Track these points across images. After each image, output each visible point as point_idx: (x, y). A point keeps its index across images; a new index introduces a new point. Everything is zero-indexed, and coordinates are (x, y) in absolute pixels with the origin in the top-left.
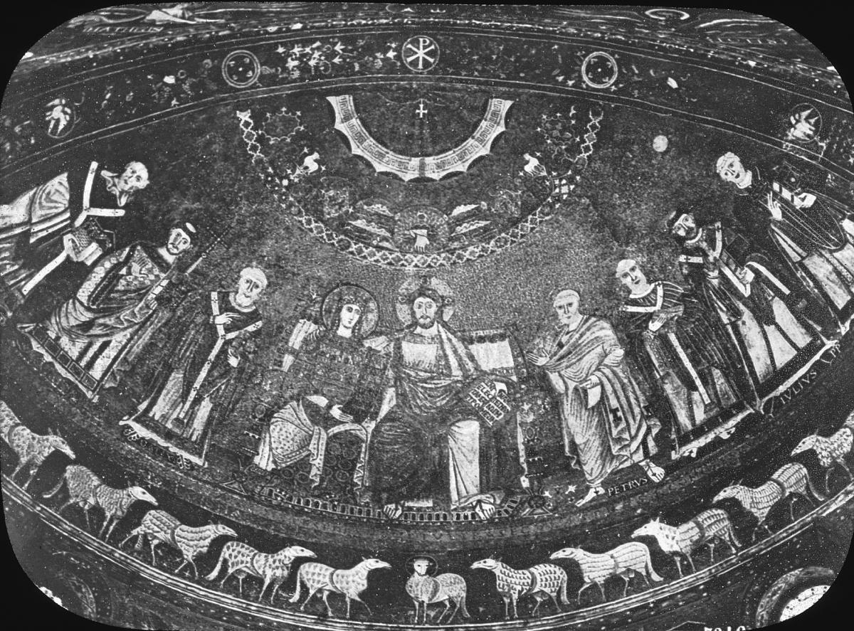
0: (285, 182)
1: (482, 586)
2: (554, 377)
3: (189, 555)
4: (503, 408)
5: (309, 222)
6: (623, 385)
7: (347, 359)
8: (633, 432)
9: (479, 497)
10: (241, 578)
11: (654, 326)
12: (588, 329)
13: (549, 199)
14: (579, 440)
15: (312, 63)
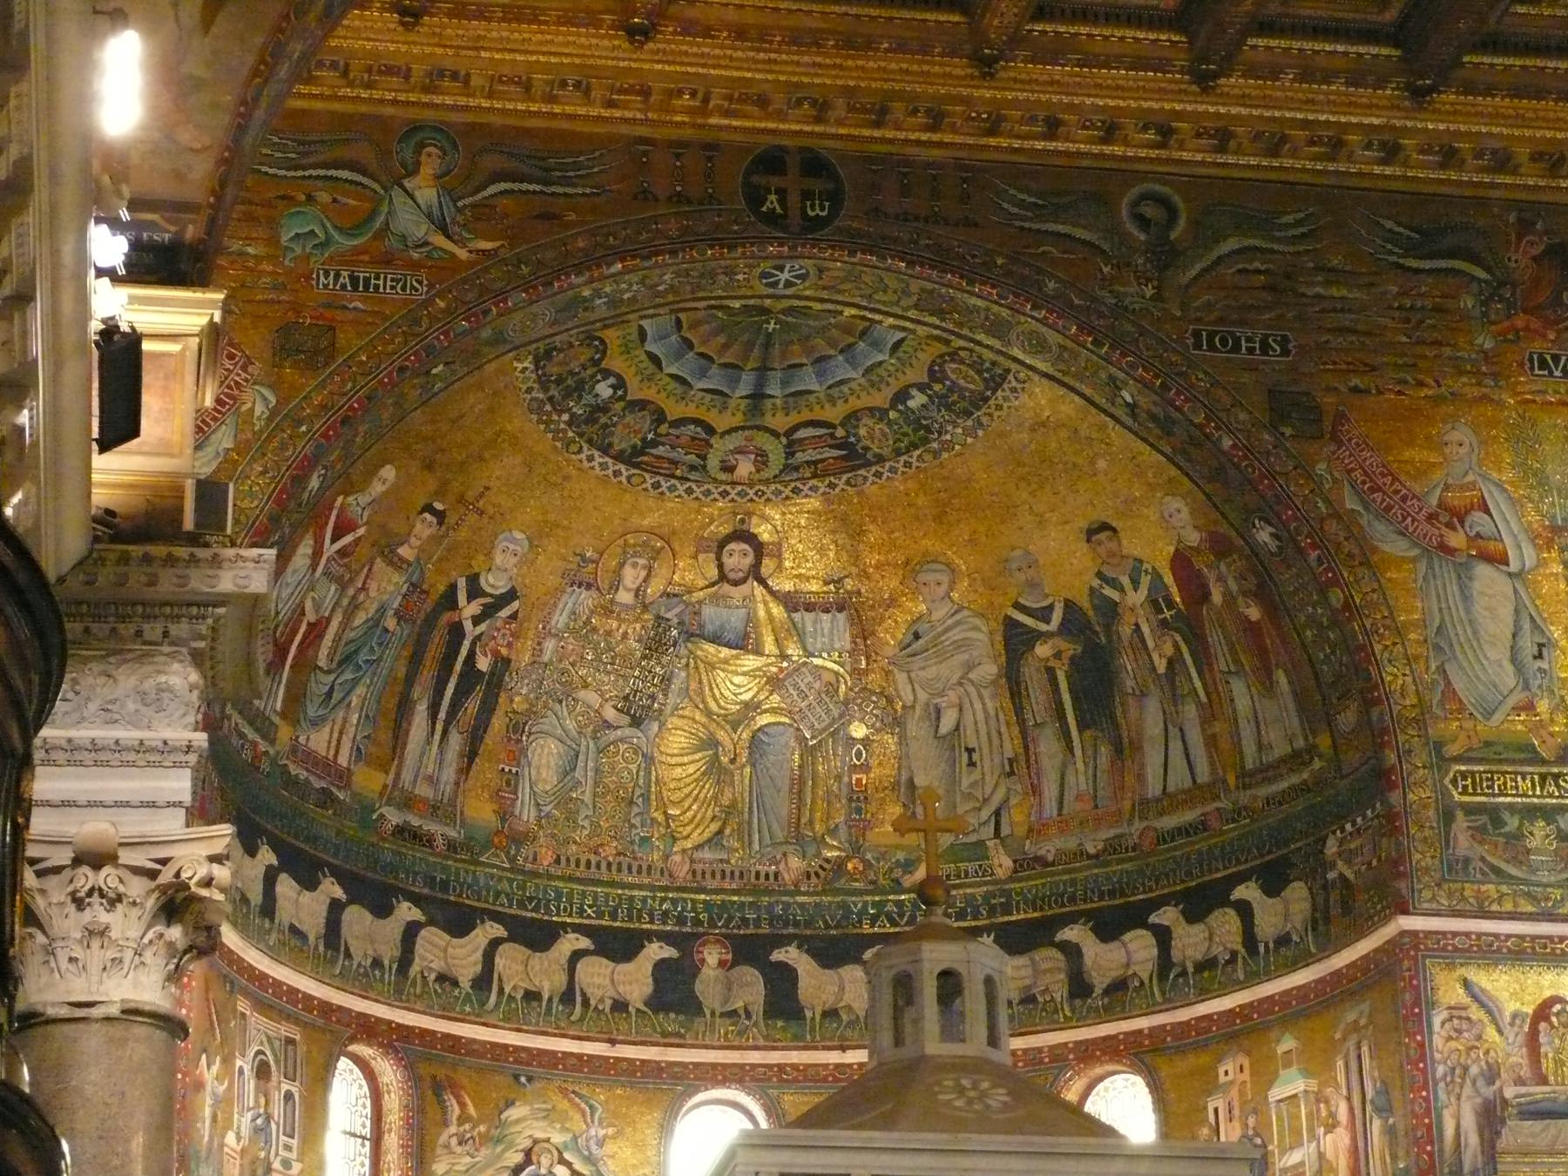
0: (565, 417)
1: (782, 984)
2: (901, 677)
3: (465, 984)
4: (828, 712)
5: (590, 459)
6: (987, 718)
7: (626, 633)
8: (988, 790)
9: (784, 848)
10: (519, 997)
11: (1043, 650)
12: (958, 623)
13: (935, 445)
14: (916, 781)
15: (626, 296)
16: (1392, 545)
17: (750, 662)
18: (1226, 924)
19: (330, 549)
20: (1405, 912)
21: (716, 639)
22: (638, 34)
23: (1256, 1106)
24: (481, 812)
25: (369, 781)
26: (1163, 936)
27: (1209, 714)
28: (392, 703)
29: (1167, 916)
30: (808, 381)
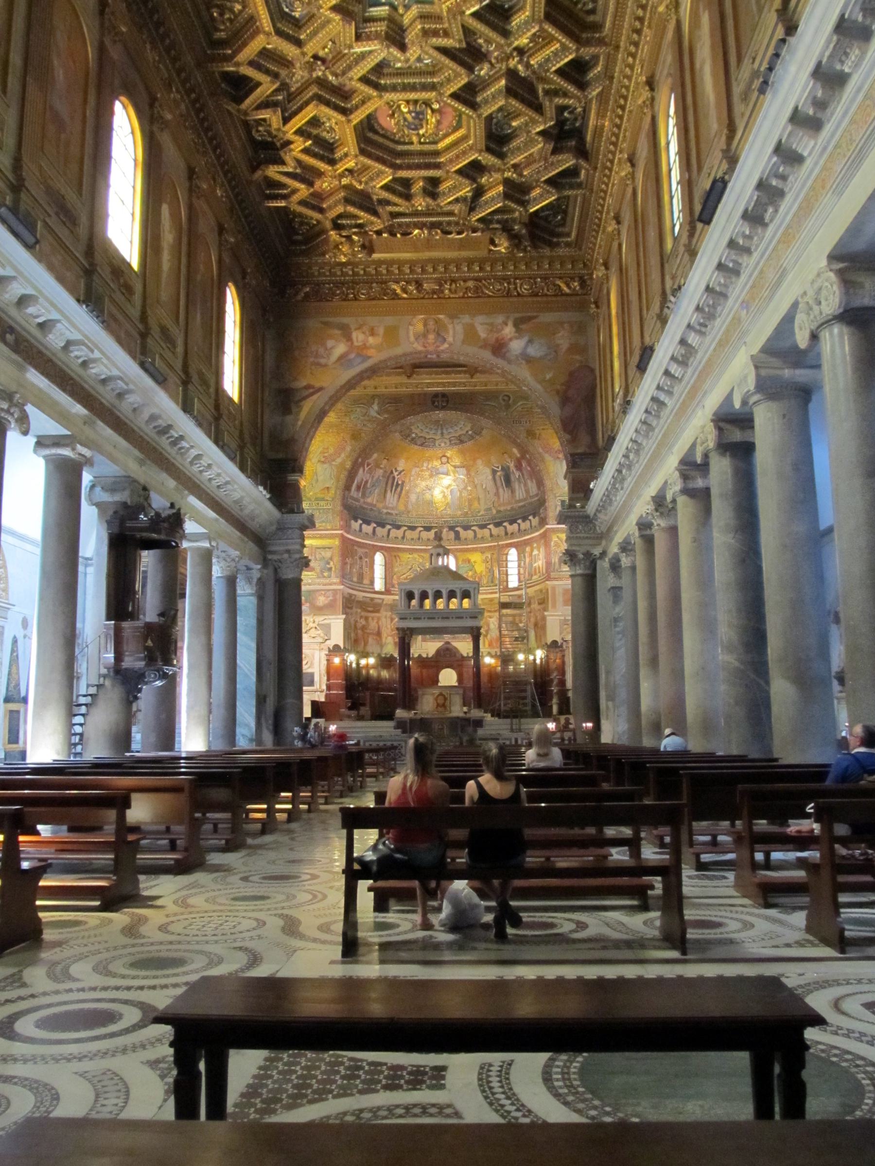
1: (457, 534)
11: (499, 474)
16: (547, 457)
17: (449, 477)
18: (528, 522)
19: (366, 469)
20: (547, 524)
21: (443, 474)
22: (409, 377)
23: (531, 555)
24: (401, 507)
25: (380, 505)
26: (519, 525)
27: (525, 485)
28: (383, 491)
29: (519, 521)
30: (450, 430)
